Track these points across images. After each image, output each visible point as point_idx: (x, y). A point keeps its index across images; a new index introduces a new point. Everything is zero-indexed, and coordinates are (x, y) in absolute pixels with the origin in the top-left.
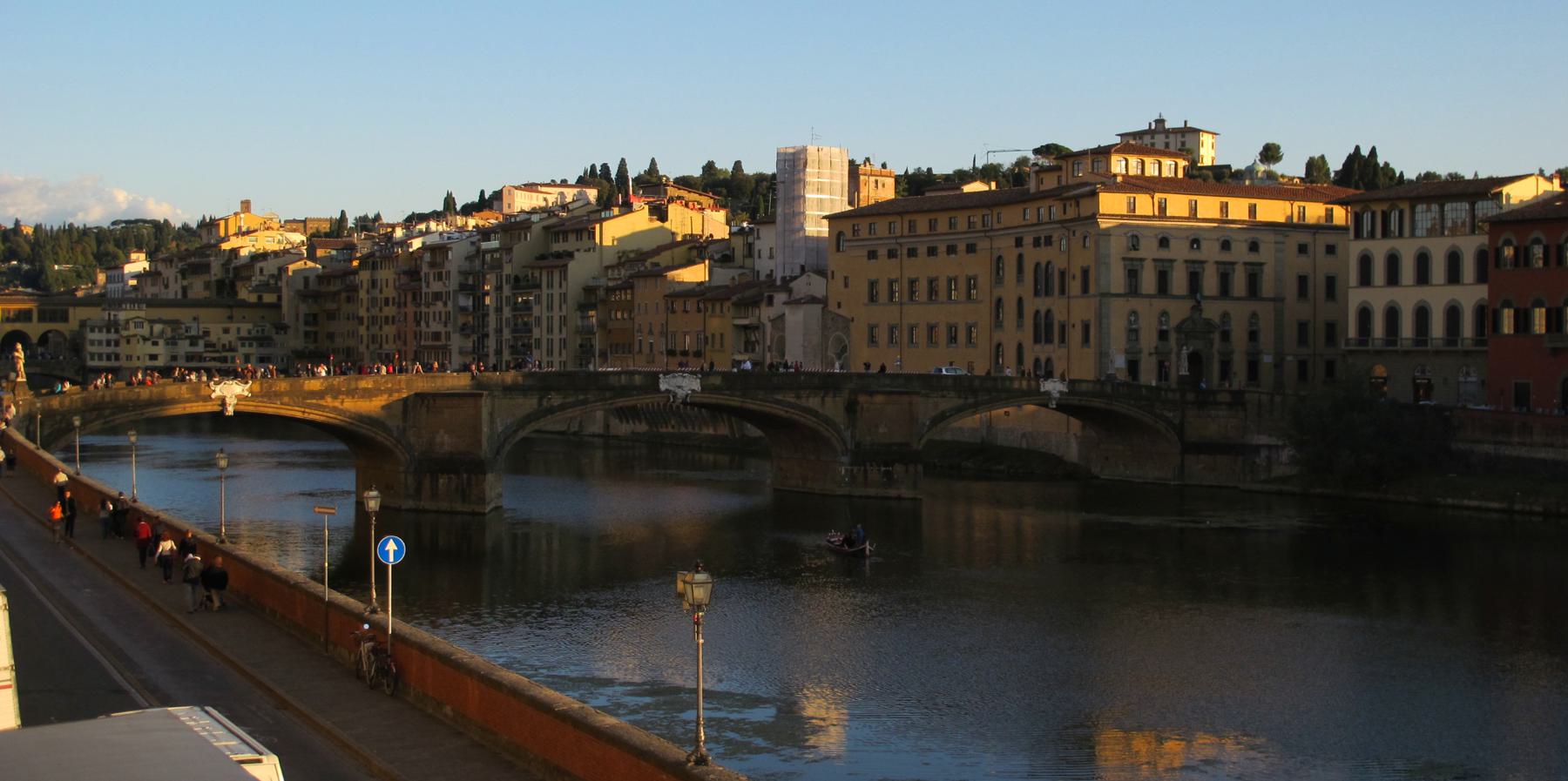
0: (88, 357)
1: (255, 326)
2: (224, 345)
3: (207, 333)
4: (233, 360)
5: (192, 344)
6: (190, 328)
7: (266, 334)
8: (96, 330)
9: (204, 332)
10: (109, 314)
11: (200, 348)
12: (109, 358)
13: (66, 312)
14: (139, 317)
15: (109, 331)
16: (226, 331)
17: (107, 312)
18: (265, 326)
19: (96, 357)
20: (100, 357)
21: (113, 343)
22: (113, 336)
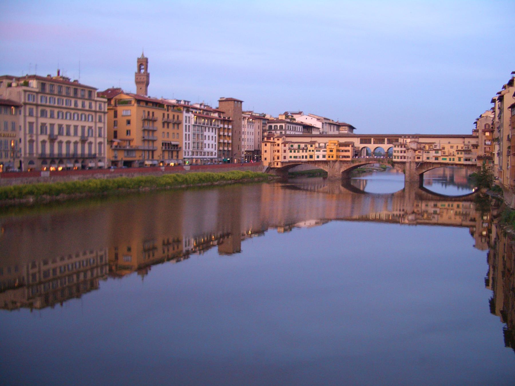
0: (393, 157)
1: (465, 145)
2: (451, 153)
3: (444, 148)
4: (454, 160)
5: (436, 153)
6: (436, 146)
7: (470, 149)
8: (397, 146)
9: (442, 147)
10: (403, 140)
11: (440, 153)
12: (401, 158)
13: (398, 139)
14: (413, 141)
15: (401, 147)
16: (452, 147)
17: (402, 139)
18: (469, 145)
19: (396, 157)
20: (398, 157)
21: (403, 152)
22: (403, 149)
